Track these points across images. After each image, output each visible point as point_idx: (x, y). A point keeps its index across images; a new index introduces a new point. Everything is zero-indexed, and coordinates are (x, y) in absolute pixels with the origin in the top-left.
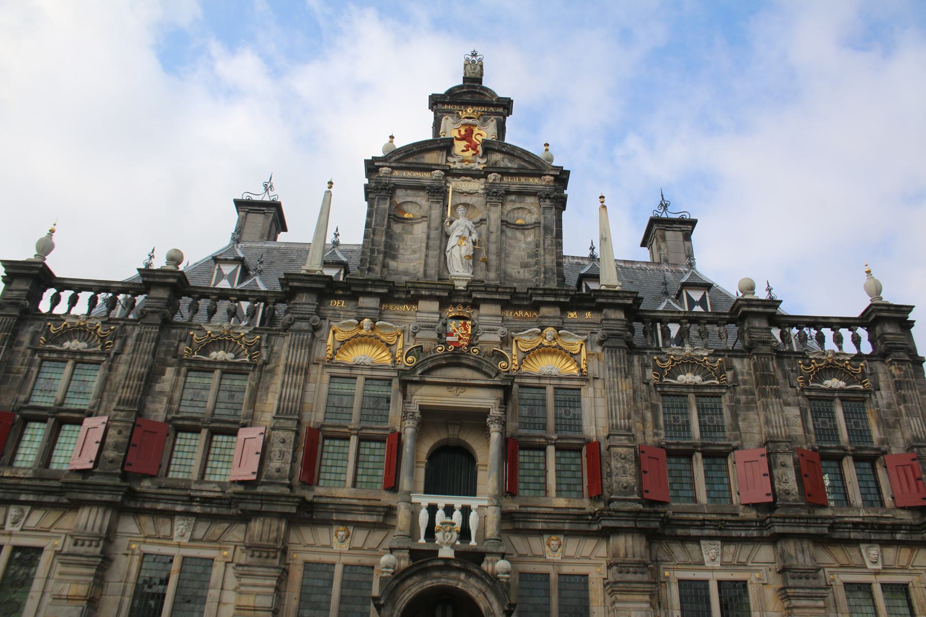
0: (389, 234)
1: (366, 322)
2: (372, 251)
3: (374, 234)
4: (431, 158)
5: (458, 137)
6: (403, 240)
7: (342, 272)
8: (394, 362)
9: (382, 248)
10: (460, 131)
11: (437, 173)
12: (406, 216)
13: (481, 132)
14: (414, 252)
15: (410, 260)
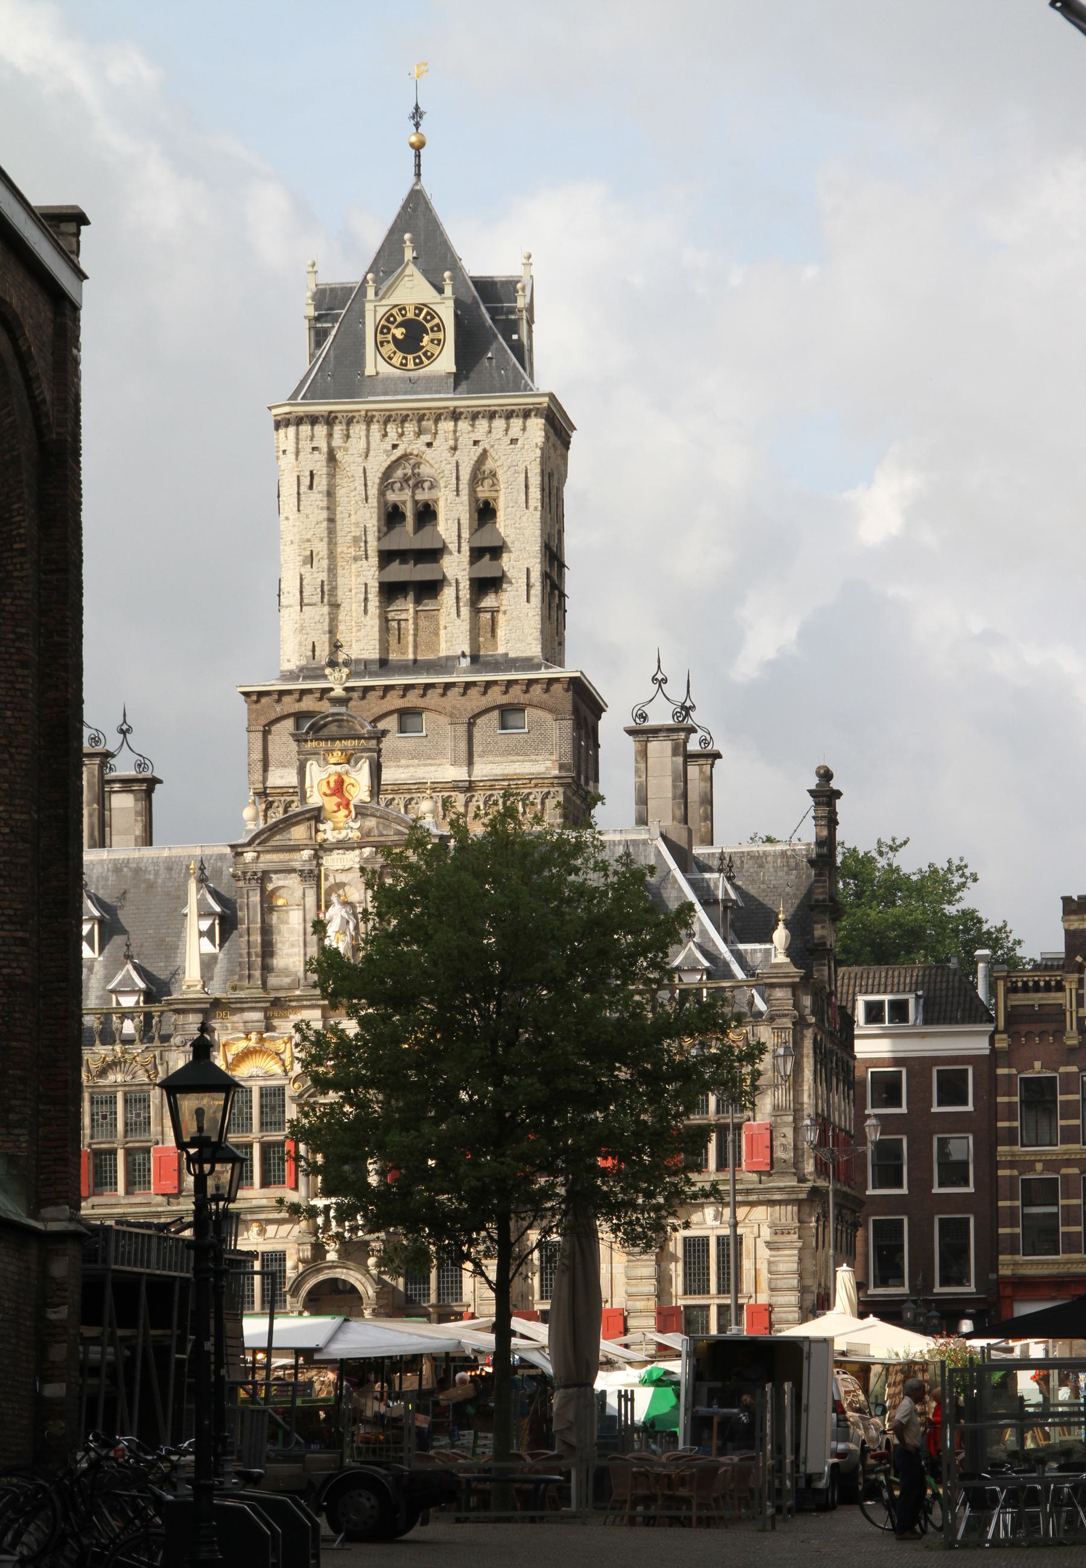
0: (267, 931)
1: (253, 1036)
2: (249, 954)
3: (249, 934)
4: (299, 833)
5: (328, 792)
6: (280, 932)
7: (217, 922)
8: (285, 1071)
9: (259, 950)
10: (328, 783)
11: (306, 854)
12: (280, 902)
13: (352, 781)
14: (293, 945)
15: (289, 955)
